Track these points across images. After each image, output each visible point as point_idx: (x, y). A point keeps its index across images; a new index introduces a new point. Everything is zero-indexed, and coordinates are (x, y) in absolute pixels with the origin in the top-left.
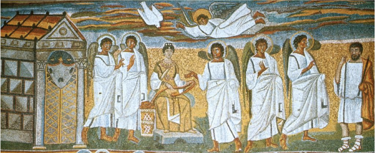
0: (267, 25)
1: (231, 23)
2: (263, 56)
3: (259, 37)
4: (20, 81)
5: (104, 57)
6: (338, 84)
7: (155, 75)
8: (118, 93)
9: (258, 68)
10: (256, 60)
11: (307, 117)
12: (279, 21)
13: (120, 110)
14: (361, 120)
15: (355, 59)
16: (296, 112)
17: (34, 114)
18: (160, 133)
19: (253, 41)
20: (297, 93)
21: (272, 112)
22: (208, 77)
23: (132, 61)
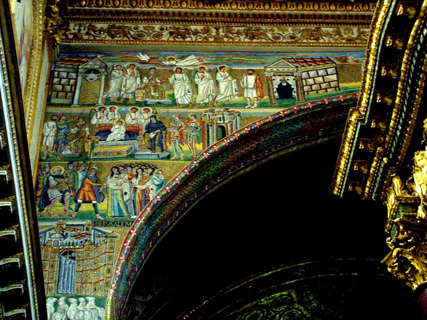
0: (205, 62)
1: (186, 61)
2: (203, 72)
3: (201, 66)
4: (67, 80)
5: (118, 71)
6: (243, 83)
7: (145, 78)
8: (124, 84)
9: (200, 76)
10: (200, 74)
11: (228, 95)
12: (211, 61)
13: (124, 90)
14: (256, 96)
15: (251, 74)
16: (222, 92)
17: (74, 92)
18: (147, 100)
19: (198, 67)
20: (222, 86)
21: (209, 93)
22: (174, 79)
23: (133, 73)
